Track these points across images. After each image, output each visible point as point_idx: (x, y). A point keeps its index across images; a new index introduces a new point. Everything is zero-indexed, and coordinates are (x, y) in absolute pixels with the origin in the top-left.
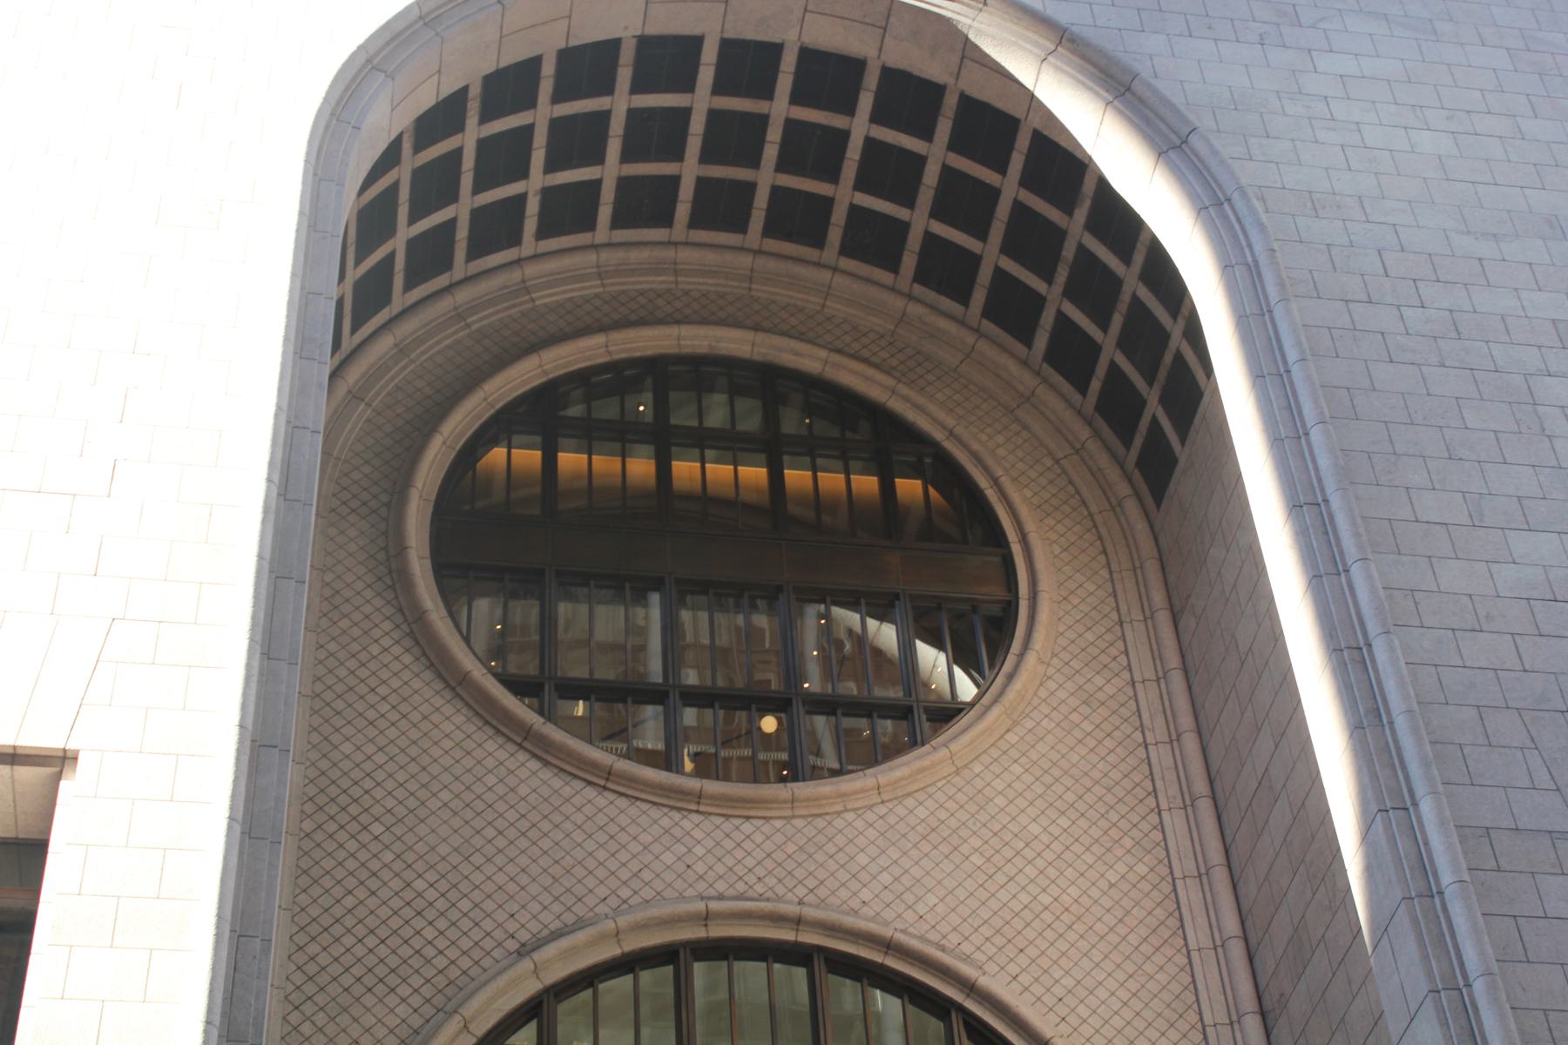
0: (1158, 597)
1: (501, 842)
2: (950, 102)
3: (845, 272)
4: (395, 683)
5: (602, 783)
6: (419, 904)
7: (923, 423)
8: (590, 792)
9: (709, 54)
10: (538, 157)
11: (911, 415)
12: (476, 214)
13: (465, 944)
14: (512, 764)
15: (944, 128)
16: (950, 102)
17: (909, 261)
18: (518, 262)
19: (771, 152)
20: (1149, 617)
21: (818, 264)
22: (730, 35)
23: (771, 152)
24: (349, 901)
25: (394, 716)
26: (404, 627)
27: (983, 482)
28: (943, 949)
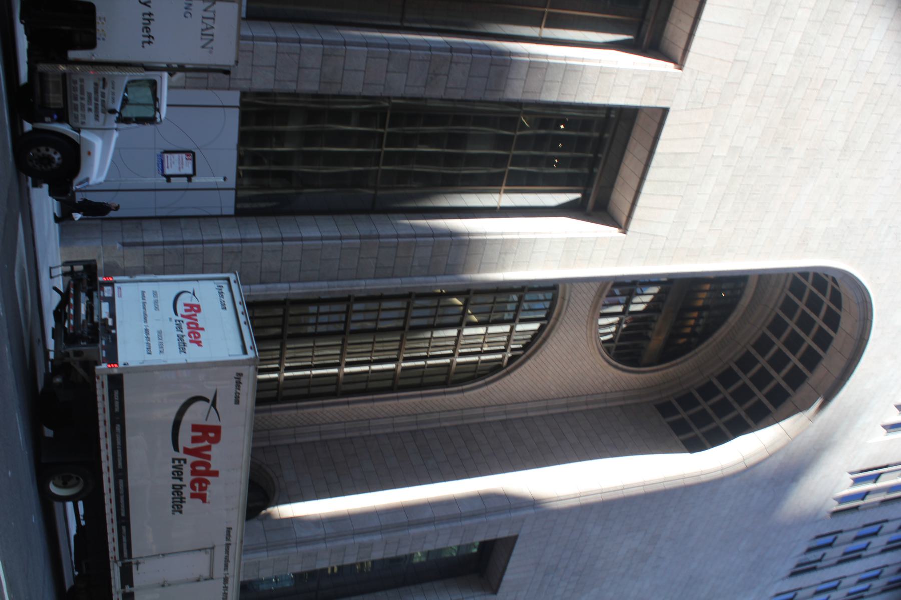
0: (629, 402)
2: (790, 391)
7: (702, 346)
11: (706, 344)
16: (790, 391)
20: (624, 399)
27: (678, 360)
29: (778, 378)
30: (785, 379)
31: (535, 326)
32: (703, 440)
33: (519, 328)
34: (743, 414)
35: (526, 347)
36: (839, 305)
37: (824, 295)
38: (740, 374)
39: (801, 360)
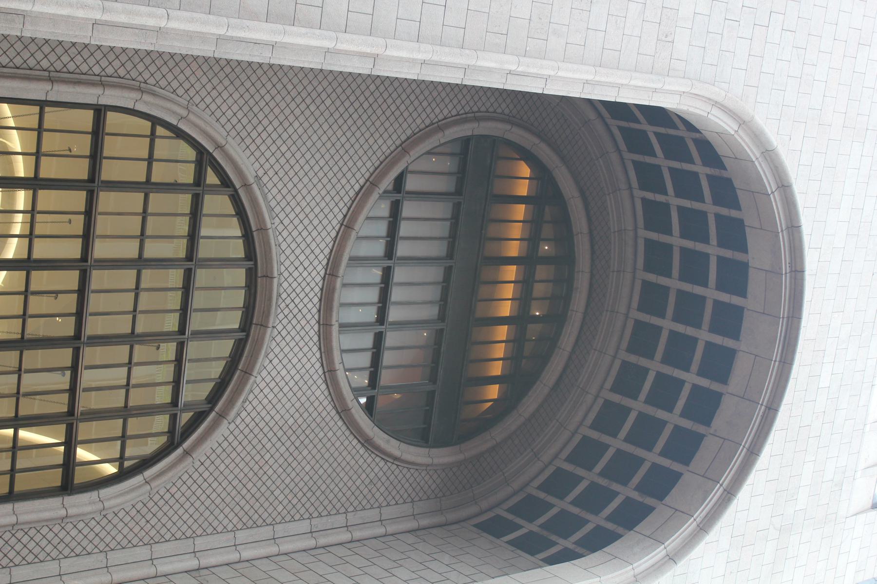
1: (316, 168)
3: (613, 362)
4: (406, 114)
6: (286, 124)
8: (340, 217)
9: (736, 300)
10: (686, 203)
12: (658, 168)
13: (263, 148)
14: (358, 175)
15: (686, 424)
17: (616, 398)
18: (630, 188)
19: (680, 328)
21: (618, 348)
22: (746, 312)
23: (680, 328)
24: (290, 87)
25: (388, 113)
26: (436, 120)
28: (244, 402)
32: (579, 550)
34: (635, 495)
35: (213, 398)
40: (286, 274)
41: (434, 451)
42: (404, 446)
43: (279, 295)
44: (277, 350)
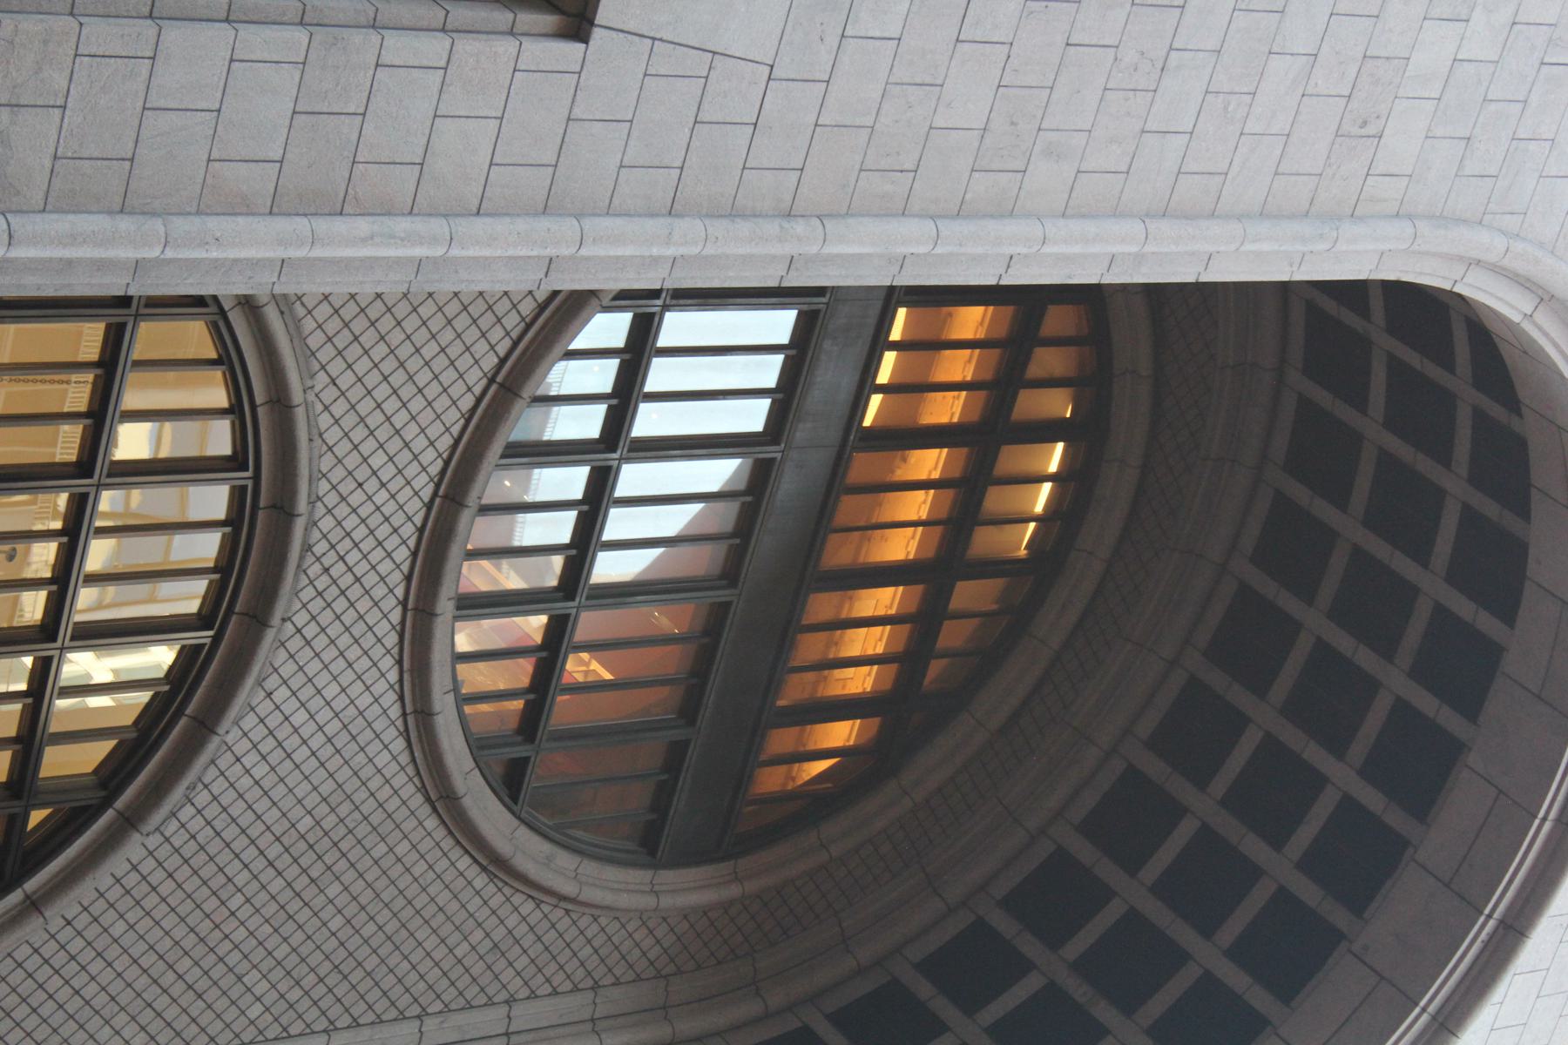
2: (1339, 917)
5: (499, 379)
8: (490, 362)
16: (1339, 917)
28: (192, 787)
29: (1280, 868)
30: (1308, 864)
31: (159, 657)
33: (82, 665)
35: (113, 775)
36: (1518, 496)
37: (1445, 460)
38: (1108, 871)
39: (1370, 771)
40: (331, 500)
41: (668, 876)
42: (590, 868)
43: (307, 548)
44: (288, 669)
